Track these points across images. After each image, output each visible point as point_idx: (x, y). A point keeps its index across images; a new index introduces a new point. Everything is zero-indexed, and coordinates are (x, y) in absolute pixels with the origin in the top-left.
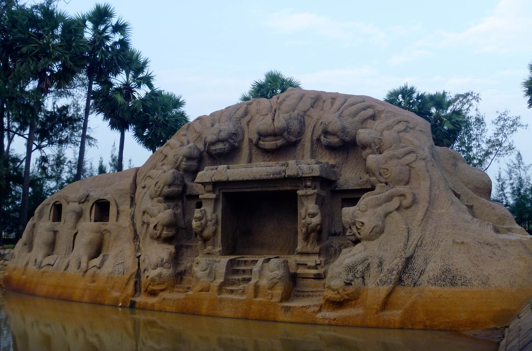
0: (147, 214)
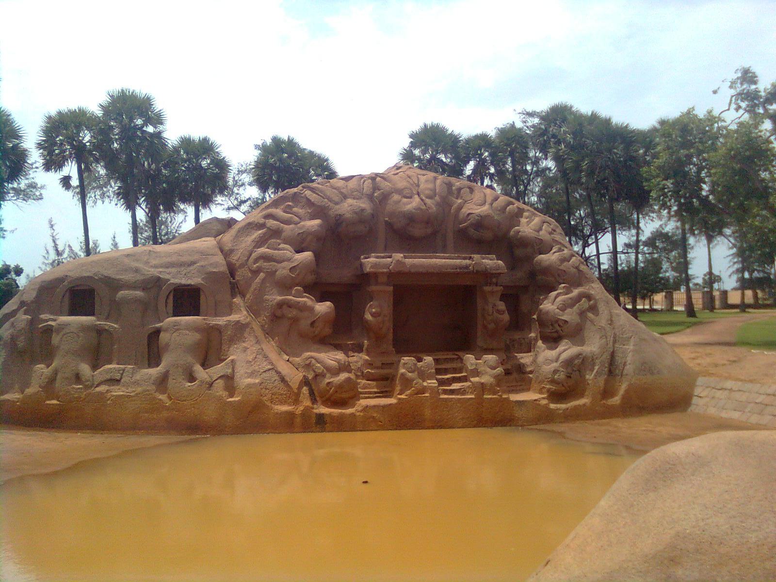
0: (290, 307)
